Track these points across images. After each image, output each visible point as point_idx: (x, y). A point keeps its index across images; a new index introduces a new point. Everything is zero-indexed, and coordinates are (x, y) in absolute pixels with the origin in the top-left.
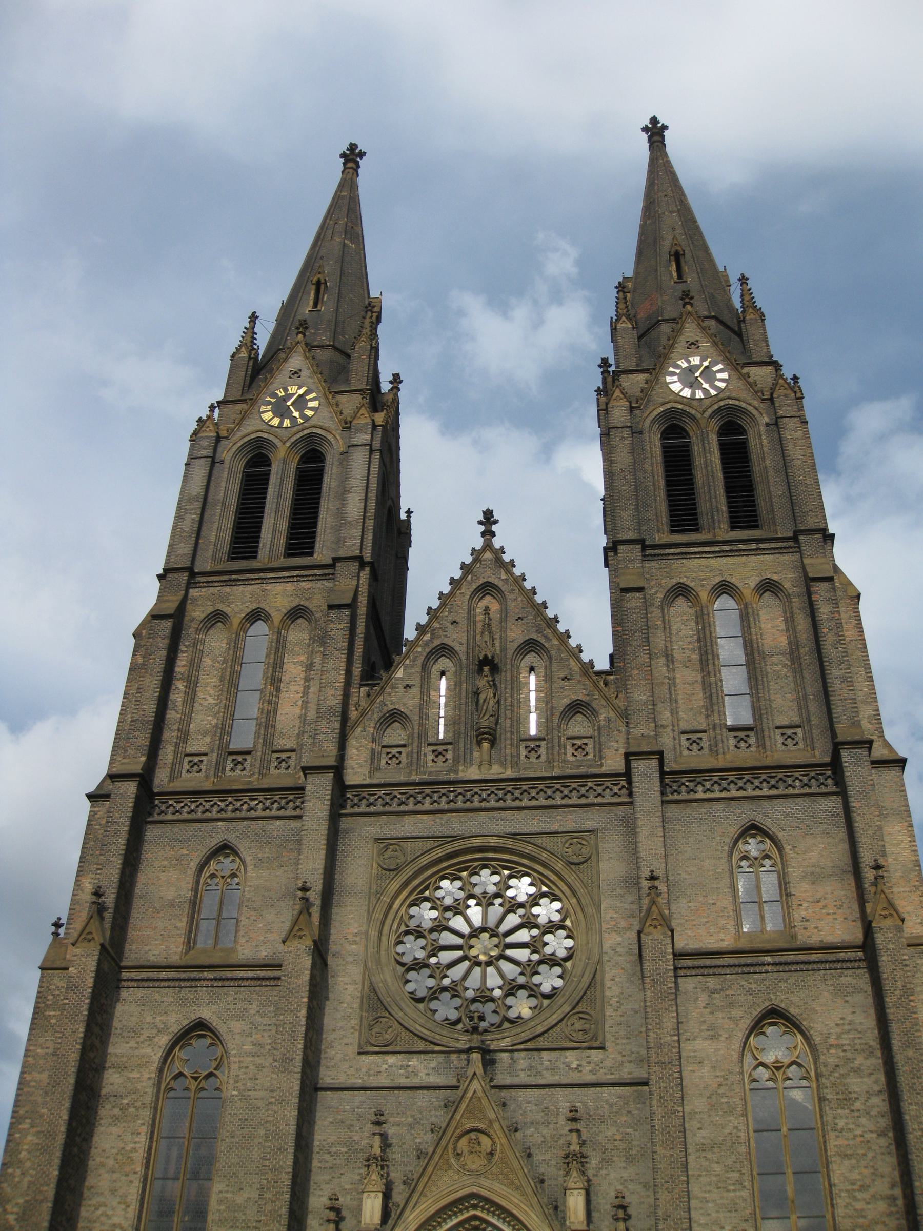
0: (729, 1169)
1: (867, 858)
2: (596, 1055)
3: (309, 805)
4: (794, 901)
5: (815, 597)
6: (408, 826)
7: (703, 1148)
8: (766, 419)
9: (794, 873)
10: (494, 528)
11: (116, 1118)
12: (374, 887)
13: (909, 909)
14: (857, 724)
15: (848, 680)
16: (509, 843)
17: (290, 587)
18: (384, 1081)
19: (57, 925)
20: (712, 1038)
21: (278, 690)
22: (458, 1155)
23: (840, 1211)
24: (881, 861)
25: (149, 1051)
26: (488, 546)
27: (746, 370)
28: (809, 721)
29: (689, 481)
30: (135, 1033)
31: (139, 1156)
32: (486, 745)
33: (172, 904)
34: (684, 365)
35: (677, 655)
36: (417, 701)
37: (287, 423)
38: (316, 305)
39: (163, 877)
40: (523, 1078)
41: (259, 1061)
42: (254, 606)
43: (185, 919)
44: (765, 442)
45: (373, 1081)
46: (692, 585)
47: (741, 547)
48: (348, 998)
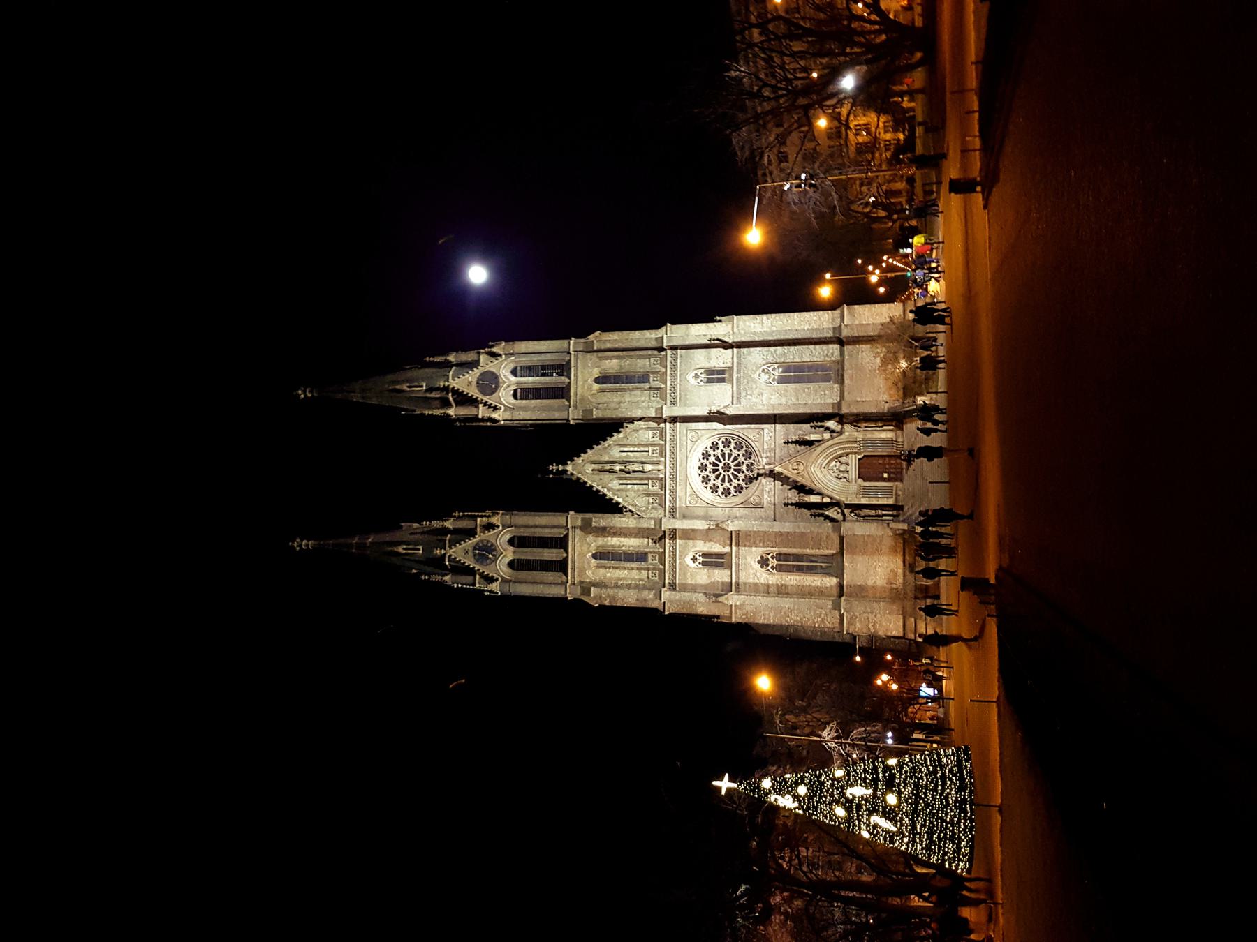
0: (804, 391)
1: (706, 341)
3: (676, 527)
4: (717, 366)
5: (603, 348)
7: (798, 399)
13: (722, 329)
17: (577, 545)
20: (762, 394)
21: (623, 546)
22: (798, 473)
23: (819, 360)
24: (709, 337)
25: (762, 579)
28: (650, 355)
29: (537, 390)
31: (798, 578)
35: (619, 399)
36: (632, 493)
41: (766, 540)
43: (715, 571)
44: (524, 359)
48: (745, 512)
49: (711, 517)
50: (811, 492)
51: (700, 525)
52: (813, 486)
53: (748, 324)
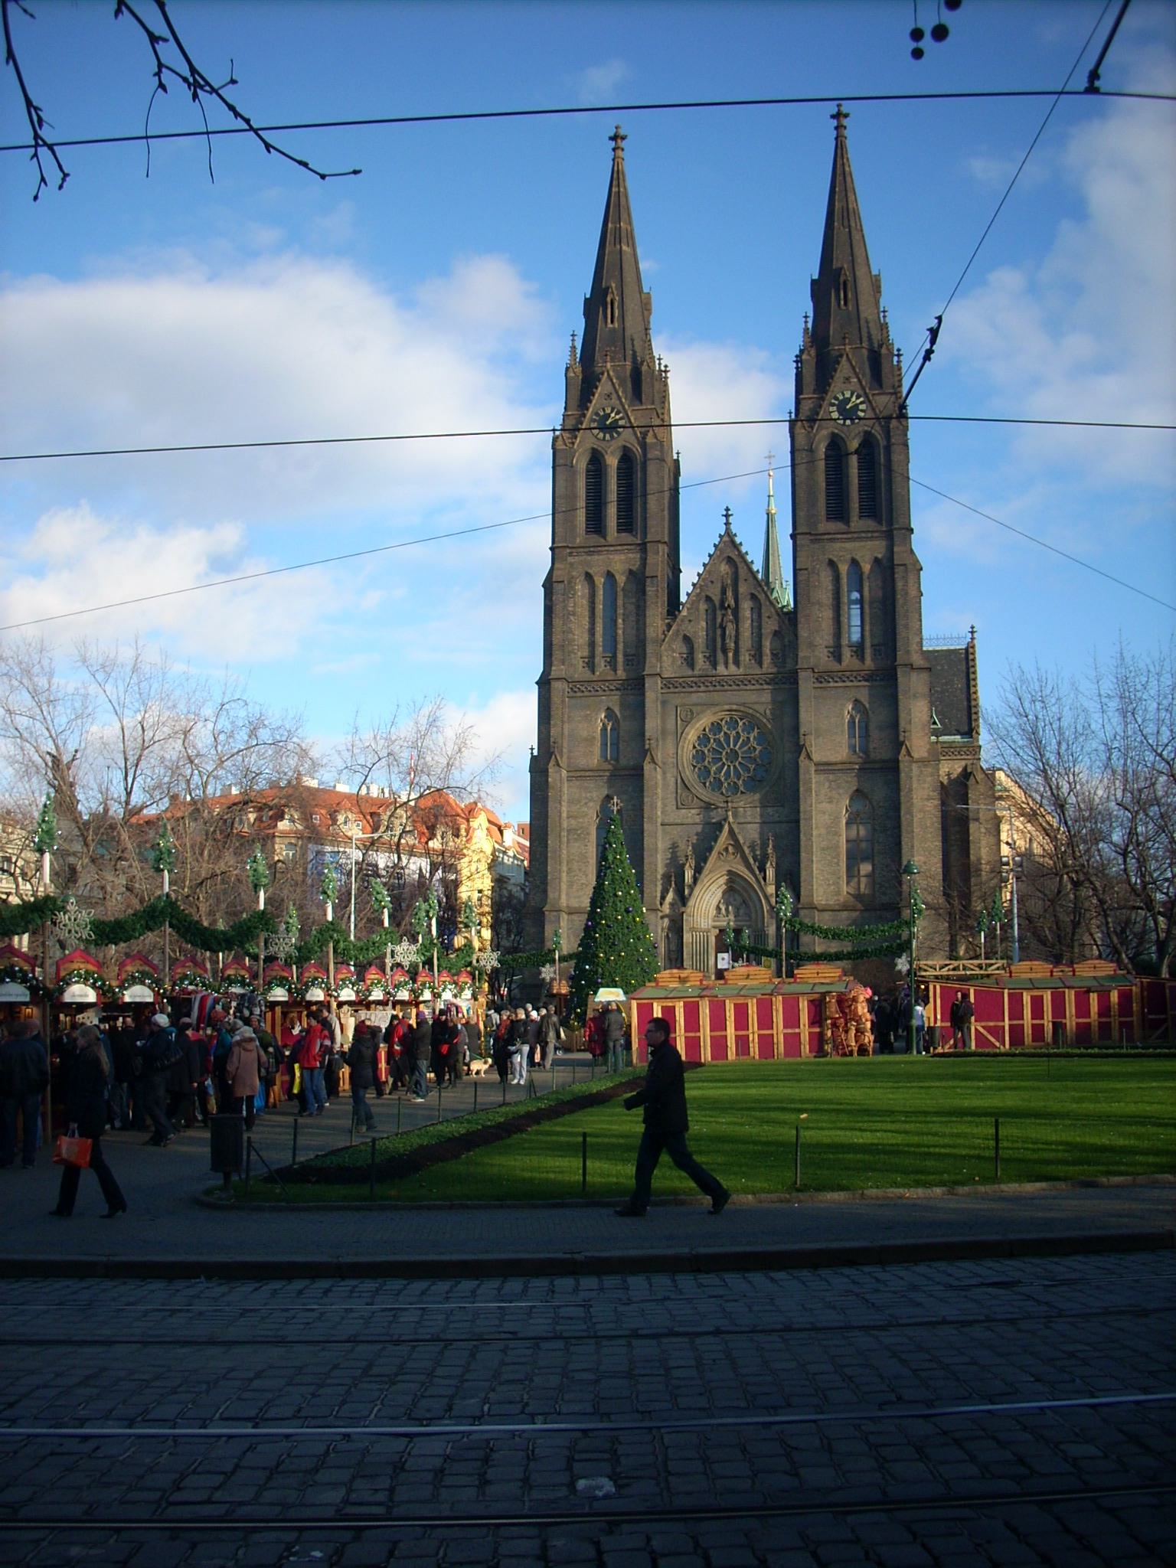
1: (902, 724)
2: (781, 809)
6: (694, 698)
8: (882, 443)
9: (872, 726)
10: (731, 519)
11: (576, 840)
12: (679, 732)
14: (908, 652)
15: (906, 626)
16: (742, 709)
17: (623, 557)
18: (690, 821)
19: (532, 749)
26: (728, 532)
27: (877, 398)
30: (579, 801)
32: (731, 655)
33: (586, 740)
34: (841, 398)
37: (608, 437)
38: (612, 322)
39: (580, 726)
40: (749, 819)
42: (605, 569)
45: (686, 821)
46: (835, 559)
47: (863, 535)
49: (664, 739)
50: (698, 870)
51: (652, 724)
52: (705, 872)
53: (929, 779)
